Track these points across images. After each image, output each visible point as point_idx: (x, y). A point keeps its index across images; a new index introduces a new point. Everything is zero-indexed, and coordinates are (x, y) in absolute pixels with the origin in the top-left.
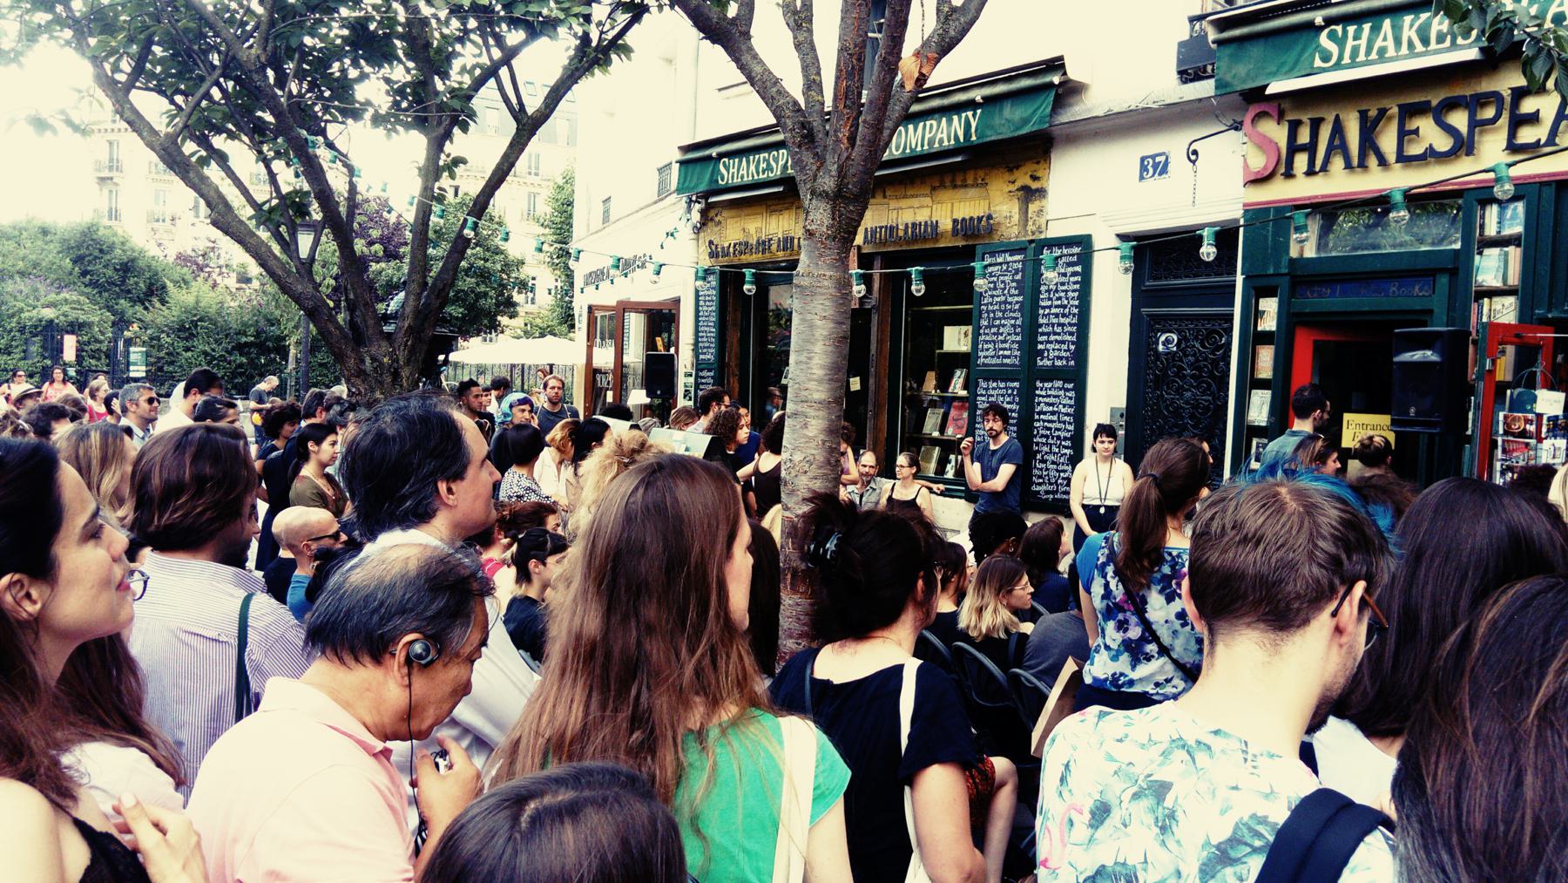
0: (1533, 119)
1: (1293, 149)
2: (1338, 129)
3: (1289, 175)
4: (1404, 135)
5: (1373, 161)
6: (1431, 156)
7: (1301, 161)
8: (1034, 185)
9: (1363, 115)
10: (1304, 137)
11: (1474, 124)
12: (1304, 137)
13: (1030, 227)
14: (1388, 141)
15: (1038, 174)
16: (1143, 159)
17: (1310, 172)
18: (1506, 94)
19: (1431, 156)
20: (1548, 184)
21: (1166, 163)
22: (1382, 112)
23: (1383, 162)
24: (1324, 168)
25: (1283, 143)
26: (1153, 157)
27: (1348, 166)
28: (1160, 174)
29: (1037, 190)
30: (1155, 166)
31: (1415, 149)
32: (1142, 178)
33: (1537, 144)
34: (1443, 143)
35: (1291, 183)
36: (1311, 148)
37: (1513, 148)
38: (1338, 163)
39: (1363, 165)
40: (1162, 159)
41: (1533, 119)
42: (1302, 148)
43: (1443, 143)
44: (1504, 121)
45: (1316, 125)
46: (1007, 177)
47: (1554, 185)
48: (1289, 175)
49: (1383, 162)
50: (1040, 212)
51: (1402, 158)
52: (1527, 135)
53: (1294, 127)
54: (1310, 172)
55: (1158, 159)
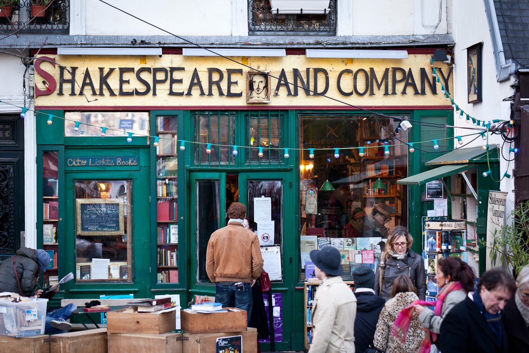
0: (180, 81)
1: (63, 81)
2: (87, 74)
4: (122, 82)
5: (106, 92)
7: (67, 87)
9: (101, 70)
10: (67, 76)
11: (156, 82)
12: (67, 76)
14: (114, 82)
17: (73, 94)
18: (168, 69)
20: (187, 110)
22: (112, 70)
23: (112, 94)
24: (81, 94)
25: (57, 78)
33: (181, 94)
34: (142, 88)
35: (62, 98)
36: (72, 82)
37: (172, 93)
38: (88, 90)
39: (101, 94)
41: (180, 81)
42: (67, 81)
43: (142, 88)
44: (168, 82)
45: (74, 69)
47: (189, 111)
48: (61, 94)
49: (112, 94)
51: (122, 93)
52: (177, 88)
53: (62, 69)
54: (73, 94)
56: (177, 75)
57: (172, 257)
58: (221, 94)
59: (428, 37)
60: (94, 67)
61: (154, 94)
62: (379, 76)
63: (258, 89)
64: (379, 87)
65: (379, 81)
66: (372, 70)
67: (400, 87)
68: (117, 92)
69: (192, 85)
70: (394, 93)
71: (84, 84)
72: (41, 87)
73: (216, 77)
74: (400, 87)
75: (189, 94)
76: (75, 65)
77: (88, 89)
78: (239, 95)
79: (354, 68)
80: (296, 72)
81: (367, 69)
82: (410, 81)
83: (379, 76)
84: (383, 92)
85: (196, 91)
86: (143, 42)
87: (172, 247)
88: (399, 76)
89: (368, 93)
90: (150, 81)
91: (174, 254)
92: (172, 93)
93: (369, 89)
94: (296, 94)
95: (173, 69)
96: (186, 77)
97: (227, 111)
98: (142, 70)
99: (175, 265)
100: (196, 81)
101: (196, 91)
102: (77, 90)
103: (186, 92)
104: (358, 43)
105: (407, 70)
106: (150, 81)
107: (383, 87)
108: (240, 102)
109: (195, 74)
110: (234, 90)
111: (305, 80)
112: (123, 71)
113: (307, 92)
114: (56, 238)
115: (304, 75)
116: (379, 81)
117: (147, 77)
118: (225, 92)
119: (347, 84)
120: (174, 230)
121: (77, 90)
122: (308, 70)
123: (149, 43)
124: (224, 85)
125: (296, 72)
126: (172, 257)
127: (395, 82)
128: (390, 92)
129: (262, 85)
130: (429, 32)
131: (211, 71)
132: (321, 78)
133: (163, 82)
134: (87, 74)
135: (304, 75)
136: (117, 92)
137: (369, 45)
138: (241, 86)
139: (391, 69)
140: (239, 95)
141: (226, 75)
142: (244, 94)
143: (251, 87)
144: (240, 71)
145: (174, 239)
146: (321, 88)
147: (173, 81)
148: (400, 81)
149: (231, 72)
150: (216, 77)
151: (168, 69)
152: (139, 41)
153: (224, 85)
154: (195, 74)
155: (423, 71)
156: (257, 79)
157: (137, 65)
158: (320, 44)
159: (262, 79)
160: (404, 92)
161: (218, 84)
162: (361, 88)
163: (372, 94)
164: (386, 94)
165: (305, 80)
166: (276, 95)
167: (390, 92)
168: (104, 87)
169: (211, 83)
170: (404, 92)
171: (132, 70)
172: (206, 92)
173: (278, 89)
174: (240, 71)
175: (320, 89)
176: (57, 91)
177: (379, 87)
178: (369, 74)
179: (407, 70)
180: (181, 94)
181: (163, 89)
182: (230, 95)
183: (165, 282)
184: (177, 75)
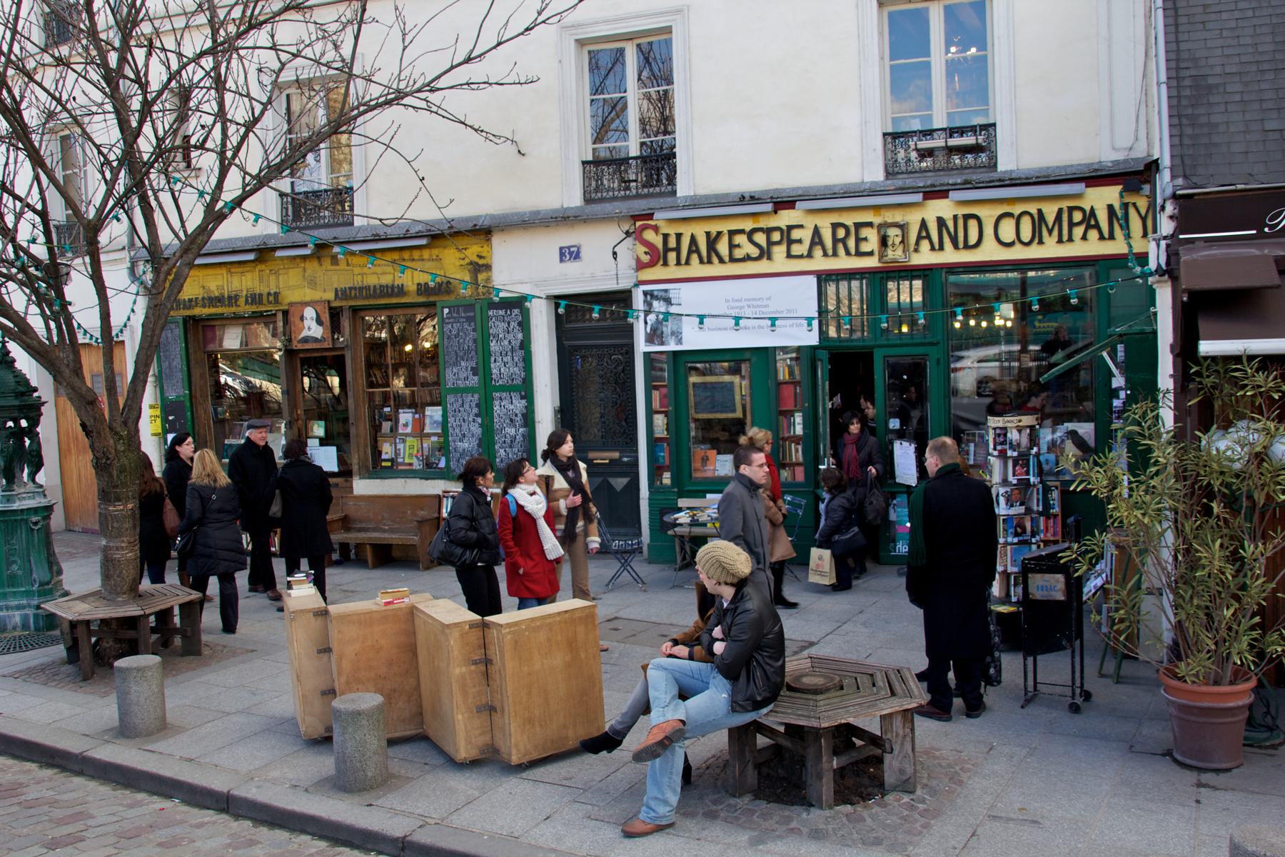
0: (800, 241)
1: (667, 249)
2: (693, 240)
3: (665, 264)
4: (732, 246)
5: (715, 259)
6: (748, 258)
7: (672, 256)
8: (481, 262)
9: (708, 234)
10: (672, 243)
11: (770, 243)
12: (672, 243)
13: (481, 290)
14: (723, 247)
15: (483, 255)
16: (561, 249)
17: (678, 263)
18: (785, 228)
19: (748, 258)
21: (578, 252)
23: (721, 261)
24: (687, 263)
25: (660, 245)
26: (569, 248)
27: (701, 262)
28: (575, 258)
29: (483, 265)
30: (571, 253)
31: (738, 253)
32: (561, 261)
33: (801, 257)
34: (754, 252)
36: (678, 249)
37: (789, 256)
39: (710, 262)
40: (575, 249)
41: (800, 241)
43: (754, 252)
45: (679, 236)
46: (458, 255)
48: (665, 264)
50: (488, 279)
51: (733, 260)
52: (796, 249)
53: (666, 236)
55: (572, 249)
56: (796, 234)
57: (797, 451)
58: (848, 253)
59: (1116, 163)
60: (700, 231)
61: (769, 258)
62: (1050, 219)
63: (893, 245)
64: (1050, 232)
65: (1050, 225)
66: (1040, 211)
67: (1078, 231)
68: (727, 259)
69: (813, 244)
70: (1070, 239)
71: (690, 252)
72: (646, 259)
73: (841, 233)
74: (1078, 231)
75: (810, 255)
76: (680, 231)
77: (695, 257)
78: (871, 254)
79: (1017, 210)
80: (941, 222)
81: (1034, 212)
82: (1093, 222)
83: (1050, 219)
84: (1056, 239)
85: (818, 252)
86: (752, 198)
87: (797, 440)
88: (1078, 217)
89: (1036, 240)
90: (763, 243)
91: (800, 448)
92: (789, 256)
93: (1037, 238)
94: (941, 248)
95: (790, 228)
96: (805, 235)
97: (858, 273)
98: (754, 231)
99: (801, 459)
100: (817, 240)
101: (818, 252)
102: (683, 261)
103: (805, 254)
104: (1019, 179)
105: (1088, 209)
106: (763, 243)
107: (1055, 233)
108: (872, 262)
109: (816, 232)
110: (865, 247)
111: (952, 230)
112: (732, 233)
113: (956, 246)
114: (667, 429)
115: (950, 224)
116: (1050, 225)
117: (760, 238)
118: (853, 251)
119: (1007, 230)
120: (798, 418)
121: (683, 261)
122: (955, 217)
123: (758, 199)
124: (851, 243)
125: (941, 222)
126: (797, 451)
127: (1072, 225)
128: (1065, 238)
129: (898, 240)
130: (1120, 156)
131: (835, 226)
132: (973, 225)
133: (779, 243)
134: (693, 240)
135: (950, 224)
136: (727, 259)
137: (1034, 180)
138: (872, 243)
139: (1065, 209)
140: (871, 254)
141: (853, 230)
142: (876, 253)
143: (884, 242)
144: (870, 225)
145: (799, 430)
146: (973, 239)
147: (791, 242)
148: (1079, 224)
149: (859, 226)
150: (841, 233)
151: (785, 228)
152: (747, 198)
153: (851, 243)
154: (816, 232)
155: (1110, 208)
156: (893, 233)
157: (748, 225)
158: (970, 183)
159: (897, 231)
160: (1084, 238)
161: (844, 241)
162: (1026, 234)
163: (1041, 242)
164: (1060, 241)
165: (952, 230)
166: (916, 250)
167: (1065, 238)
168: (713, 255)
169: (835, 241)
170: (1084, 238)
171: (741, 232)
172: (830, 252)
173: (917, 243)
174: (870, 225)
175: (973, 239)
176: (661, 262)
177: (1050, 232)
178: (1036, 217)
179: (1088, 209)
180: (801, 257)
181: (779, 251)
182: (859, 254)
183: (790, 479)
184: (796, 234)
